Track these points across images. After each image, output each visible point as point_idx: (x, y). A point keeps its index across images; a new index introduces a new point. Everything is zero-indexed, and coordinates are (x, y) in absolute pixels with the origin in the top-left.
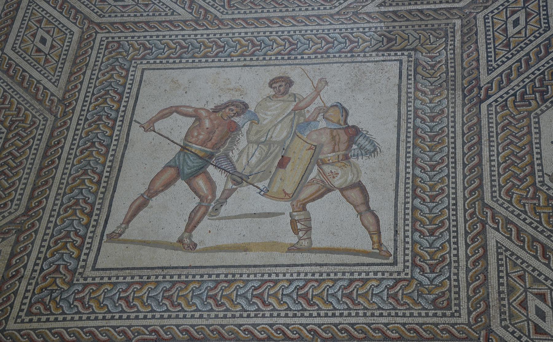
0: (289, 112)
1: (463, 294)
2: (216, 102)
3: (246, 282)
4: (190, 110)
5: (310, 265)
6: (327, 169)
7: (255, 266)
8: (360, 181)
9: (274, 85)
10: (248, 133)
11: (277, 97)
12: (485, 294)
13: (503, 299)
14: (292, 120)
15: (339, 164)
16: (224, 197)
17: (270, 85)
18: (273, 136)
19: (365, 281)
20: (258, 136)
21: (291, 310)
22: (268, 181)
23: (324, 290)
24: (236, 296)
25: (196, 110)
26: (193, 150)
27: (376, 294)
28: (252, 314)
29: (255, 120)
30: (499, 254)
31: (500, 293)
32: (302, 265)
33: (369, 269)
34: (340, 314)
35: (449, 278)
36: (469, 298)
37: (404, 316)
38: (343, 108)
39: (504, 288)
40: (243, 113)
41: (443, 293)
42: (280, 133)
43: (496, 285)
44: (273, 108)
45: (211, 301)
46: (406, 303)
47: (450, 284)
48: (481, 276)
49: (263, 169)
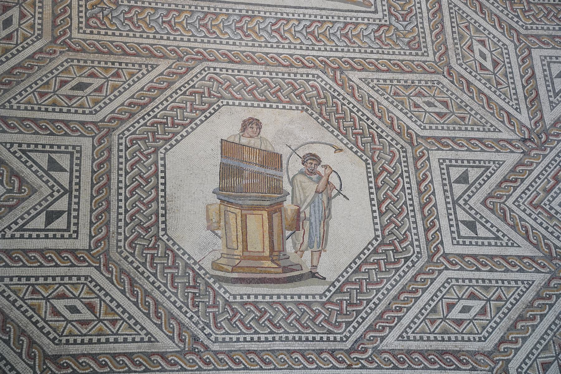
1: (428, 39)
3: (265, 18)
5: (312, 8)
7: (269, 6)
12: (444, 40)
13: (456, 44)
19: (356, 25)
21: (304, 44)
23: (326, 29)
24: (259, 30)
27: (366, 36)
28: (275, 45)
30: (450, 8)
31: (454, 39)
32: (306, 8)
33: (357, 15)
34: (342, 49)
35: (417, 26)
36: (433, 42)
37: (388, 54)
39: (456, 36)
41: (415, 37)
43: (450, 33)
45: (239, 31)
46: (388, 44)
47: (418, 30)
48: (440, 26)
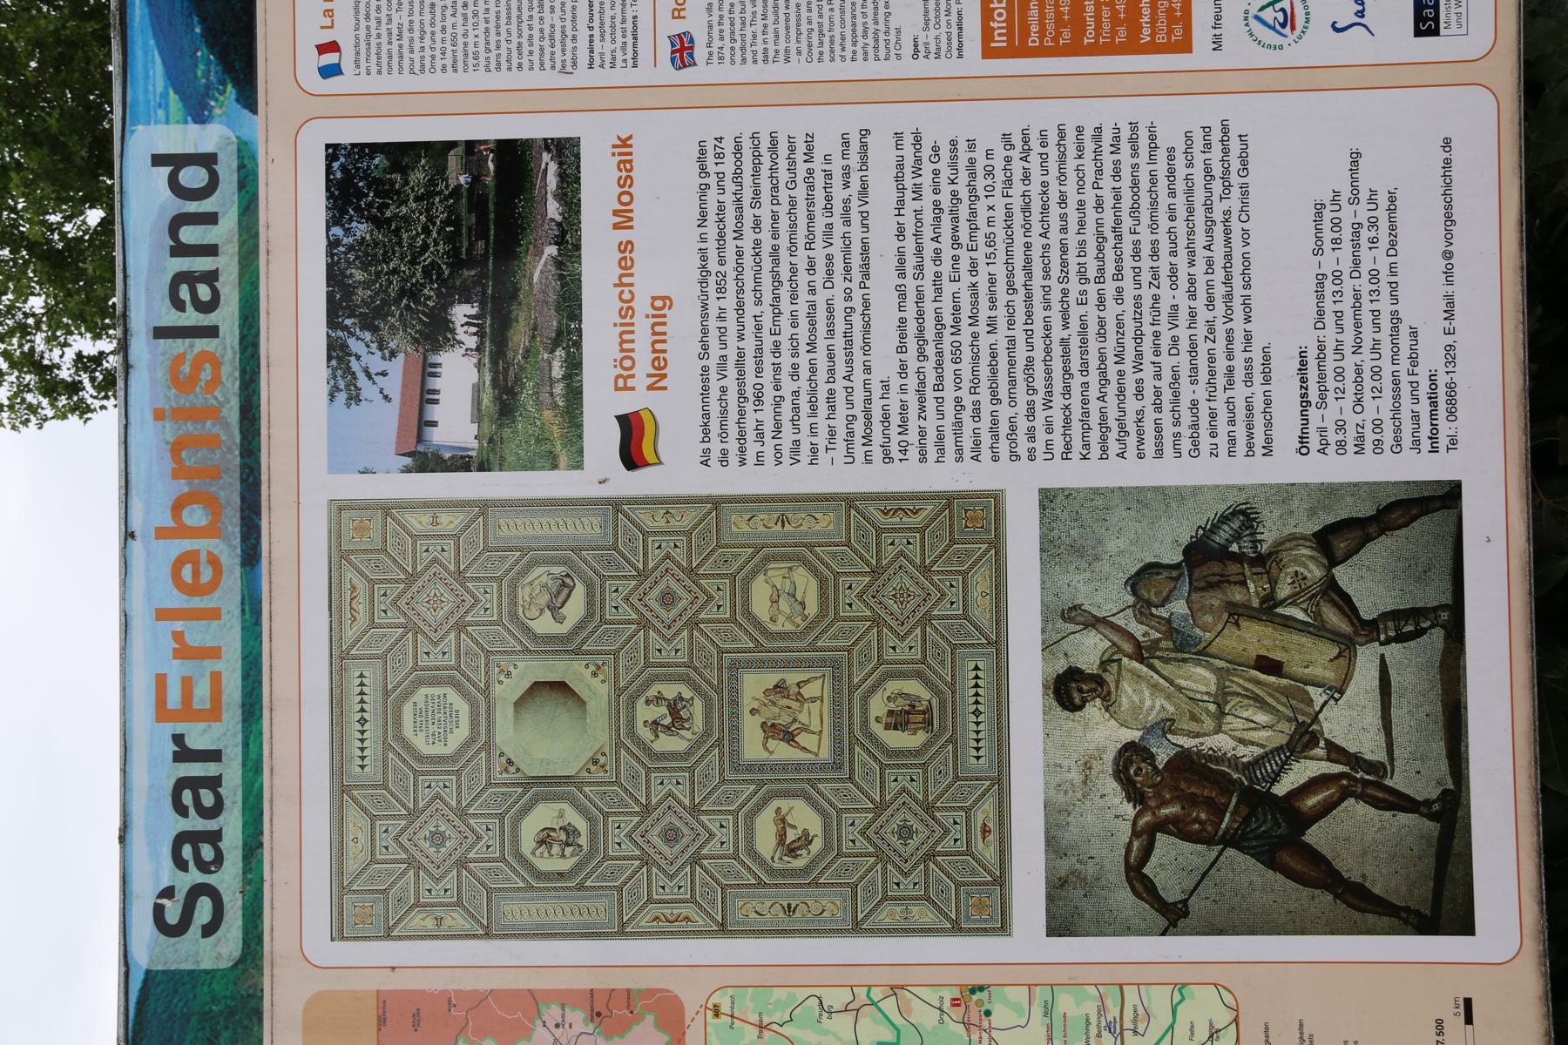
0: (1145, 669)
2: (1117, 801)
4: (1136, 844)
6: (1284, 591)
8: (1314, 535)
9: (1077, 701)
10: (1197, 735)
11: (1109, 693)
14: (1166, 661)
15: (1274, 571)
16: (1344, 759)
17: (1080, 708)
18: (1204, 689)
20: (1204, 717)
22: (1309, 688)
25: (1135, 834)
26: (1236, 825)
29: (1166, 726)
38: (1138, 573)
40: (1146, 750)
42: (1199, 678)
44: (1135, 698)
49: (1284, 700)
